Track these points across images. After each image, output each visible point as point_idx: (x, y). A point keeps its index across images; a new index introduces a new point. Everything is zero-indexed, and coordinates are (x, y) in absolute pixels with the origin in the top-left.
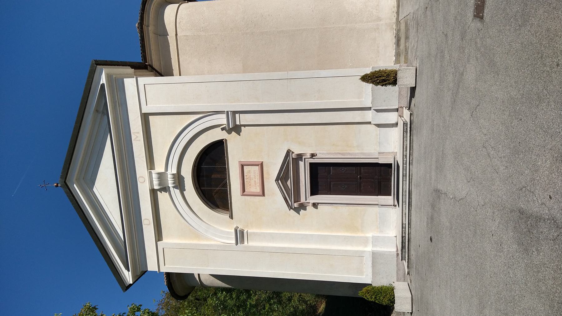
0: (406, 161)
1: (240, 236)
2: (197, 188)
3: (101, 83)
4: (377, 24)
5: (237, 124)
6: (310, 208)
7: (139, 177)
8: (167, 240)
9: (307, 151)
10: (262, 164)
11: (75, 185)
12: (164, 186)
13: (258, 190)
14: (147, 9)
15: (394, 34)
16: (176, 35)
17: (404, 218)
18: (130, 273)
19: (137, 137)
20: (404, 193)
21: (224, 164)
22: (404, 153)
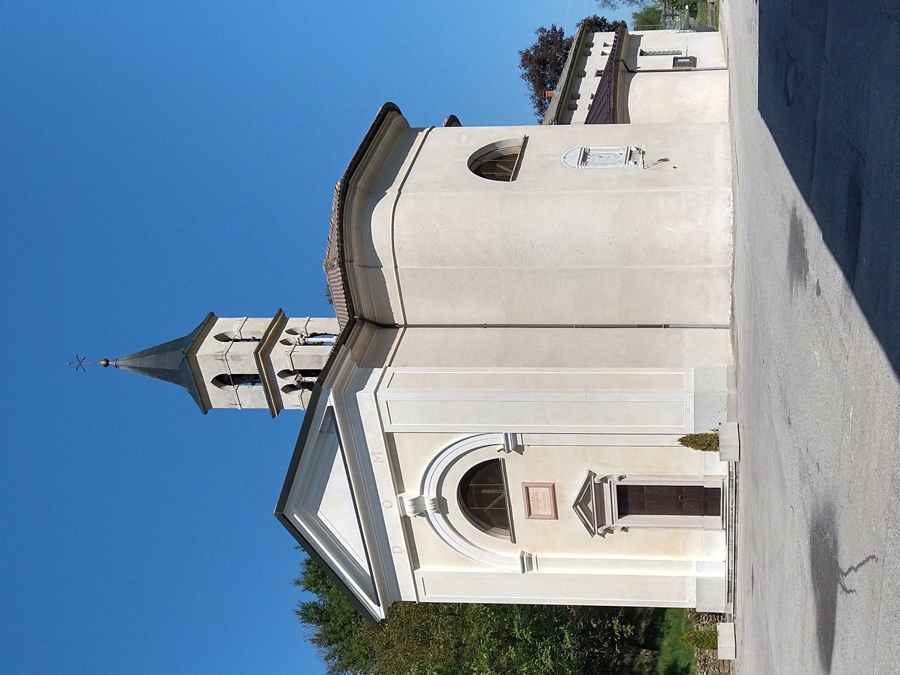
0: (733, 513)
1: (527, 563)
2: (463, 508)
3: (328, 405)
4: (706, 268)
5: (518, 444)
6: (617, 531)
7: (383, 502)
8: (425, 568)
9: (614, 473)
10: (554, 486)
11: (295, 516)
12: (421, 512)
13: (550, 512)
14: (347, 235)
15: (729, 282)
16: (396, 267)
17: (730, 554)
18: (381, 607)
19: (378, 458)
20: (730, 542)
21: (501, 488)
22: (730, 506)
